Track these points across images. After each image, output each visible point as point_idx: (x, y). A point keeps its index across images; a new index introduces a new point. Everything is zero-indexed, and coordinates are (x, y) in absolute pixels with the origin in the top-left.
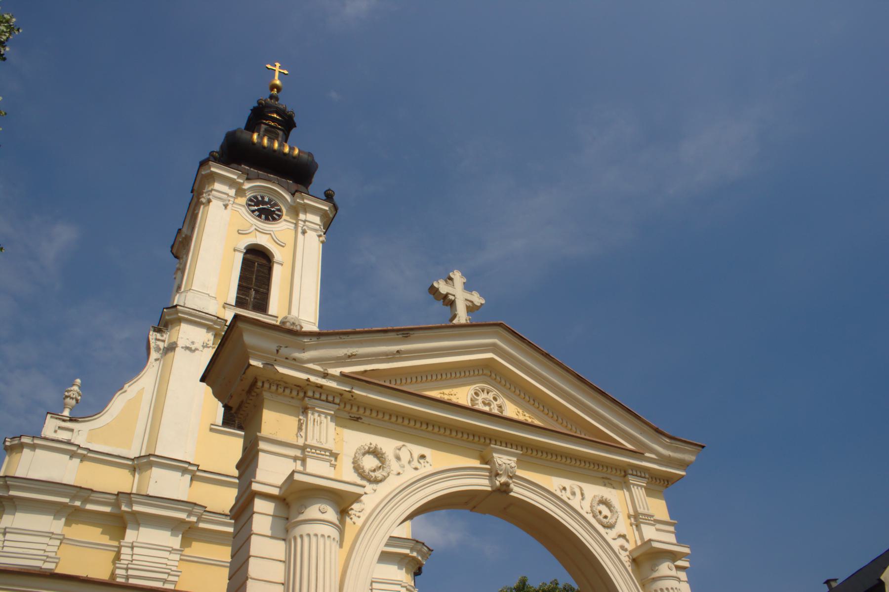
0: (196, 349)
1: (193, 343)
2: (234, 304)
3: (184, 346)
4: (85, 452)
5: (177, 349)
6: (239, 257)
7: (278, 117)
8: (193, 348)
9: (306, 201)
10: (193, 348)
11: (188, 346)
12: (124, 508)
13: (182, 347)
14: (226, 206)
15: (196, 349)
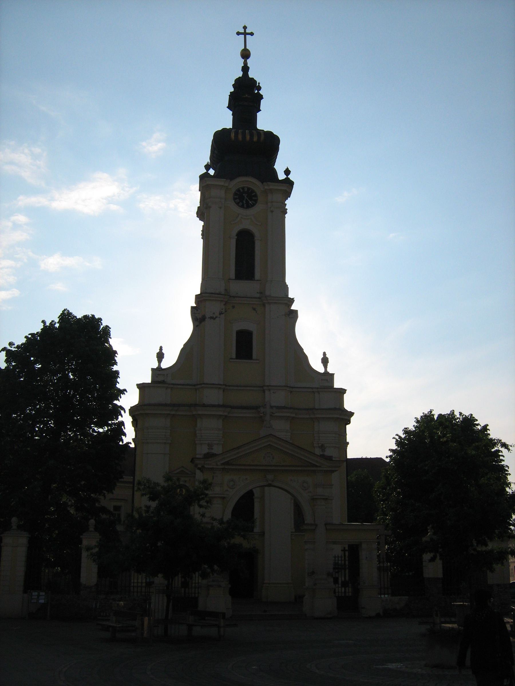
0: (216, 317)
1: (214, 313)
2: (234, 278)
3: (209, 316)
4: (172, 386)
5: (206, 320)
6: (233, 242)
7: (249, 97)
8: (214, 317)
9: (271, 187)
10: (214, 317)
11: (211, 316)
12: (194, 413)
13: (209, 318)
14: (220, 208)
15: (216, 317)
